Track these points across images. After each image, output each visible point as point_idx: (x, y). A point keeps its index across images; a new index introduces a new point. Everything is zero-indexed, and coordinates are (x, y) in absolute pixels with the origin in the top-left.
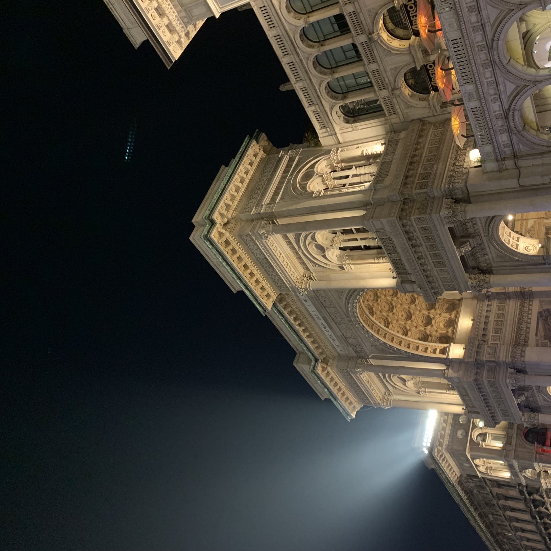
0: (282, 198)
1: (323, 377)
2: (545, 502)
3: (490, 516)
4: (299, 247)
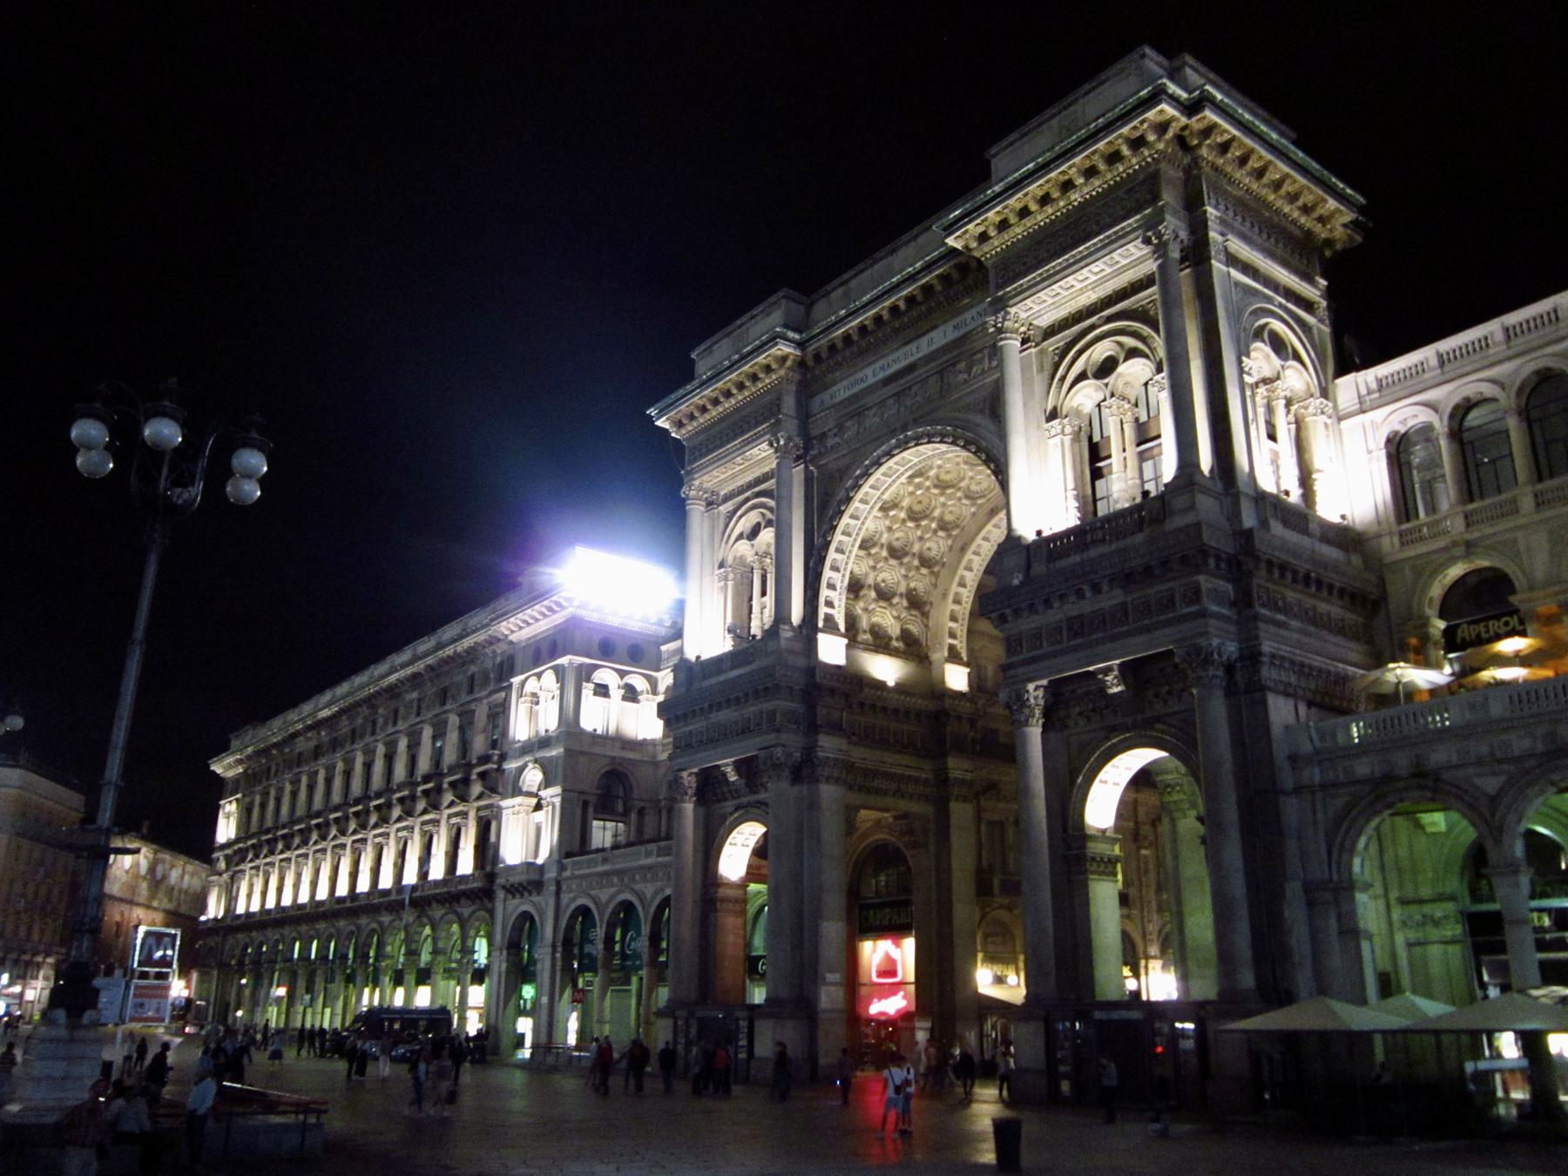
0: (1237, 284)
1: (761, 359)
2: (467, 801)
3: (415, 695)
4: (1109, 319)
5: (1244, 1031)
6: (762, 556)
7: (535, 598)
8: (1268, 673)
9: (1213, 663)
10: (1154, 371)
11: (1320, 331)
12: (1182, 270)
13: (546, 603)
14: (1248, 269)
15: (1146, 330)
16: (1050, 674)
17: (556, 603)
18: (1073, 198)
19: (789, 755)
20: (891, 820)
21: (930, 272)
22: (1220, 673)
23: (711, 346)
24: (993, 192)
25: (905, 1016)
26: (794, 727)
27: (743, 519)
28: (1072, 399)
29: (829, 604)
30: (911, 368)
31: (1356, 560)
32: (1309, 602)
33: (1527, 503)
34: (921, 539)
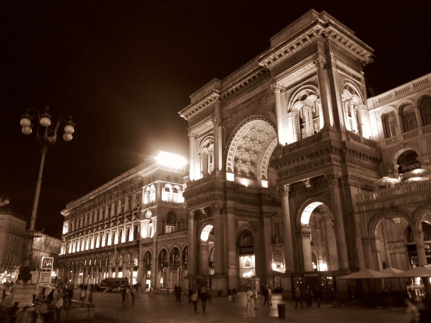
0: (339, 74)
1: (209, 98)
3: (116, 192)
4: (304, 84)
5: (346, 279)
6: (210, 152)
7: (149, 164)
8: (350, 181)
9: (335, 178)
11: (362, 86)
12: (324, 70)
13: (151, 166)
15: (315, 87)
17: (154, 166)
19: (219, 206)
20: (247, 223)
22: (337, 181)
23: (195, 95)
25: (253, 277)
27: (205, 142)
29: (229, 164)
30: (250, 99)
31: (374, 149)
32: (361, 161)
33: (421, 132)
34: (254, 146)
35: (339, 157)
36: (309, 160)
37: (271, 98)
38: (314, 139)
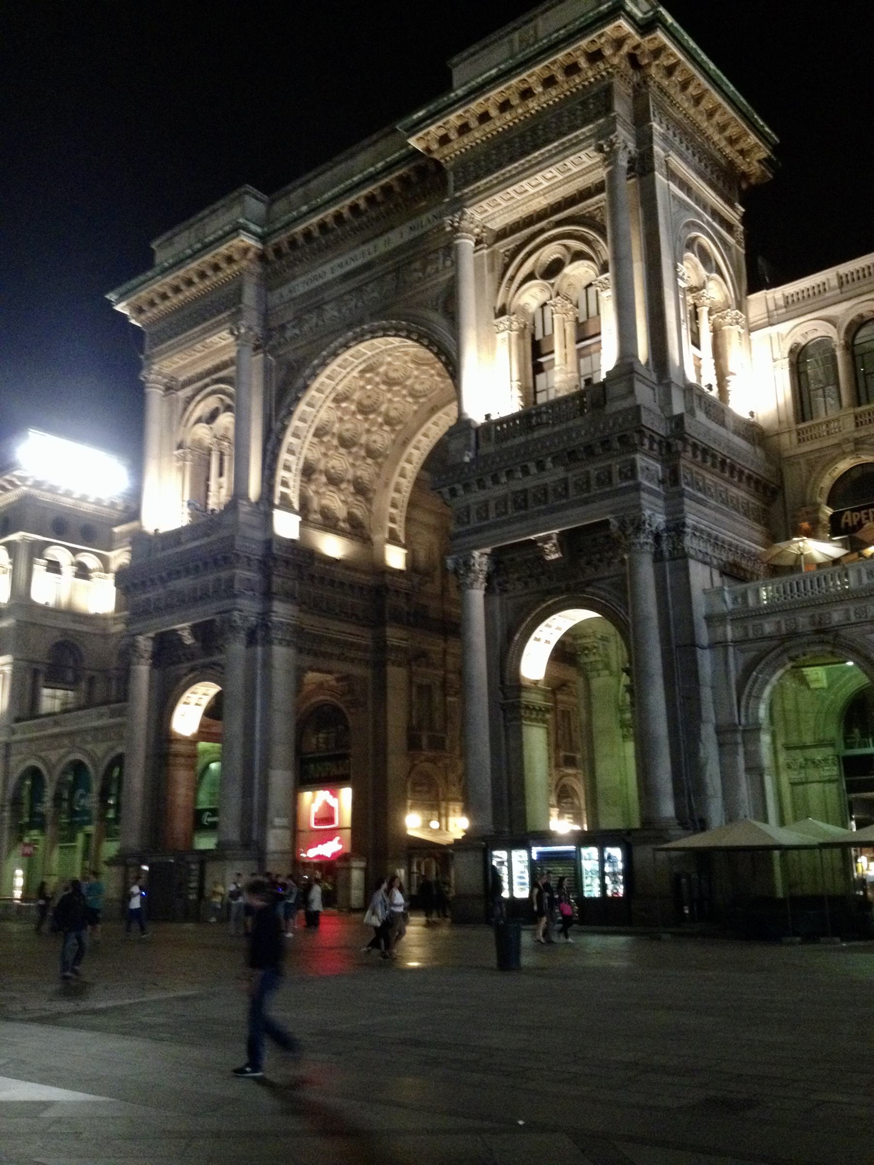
0: (675, 197)
1: (223, 249)
4: (559, 224)
8: (690, 543)
10: (598, 272)
11: (737, 251)
12: (628, 179)
14: (684, 185)
15: (592, 235)
16: (496, 542)
18: (531, 105)
20: (333, 683)
21: (391, 173)
22: (650, 541)
24: (456, 95)
26: (251, 593)
27: (202, 405)
28: (520, 297)
29: (285, 484)
30: (368, 266)
34: (368, 431)
35: (659, 466)
36: (560, 472)
37: (440, 266)
38: (582, 403)
